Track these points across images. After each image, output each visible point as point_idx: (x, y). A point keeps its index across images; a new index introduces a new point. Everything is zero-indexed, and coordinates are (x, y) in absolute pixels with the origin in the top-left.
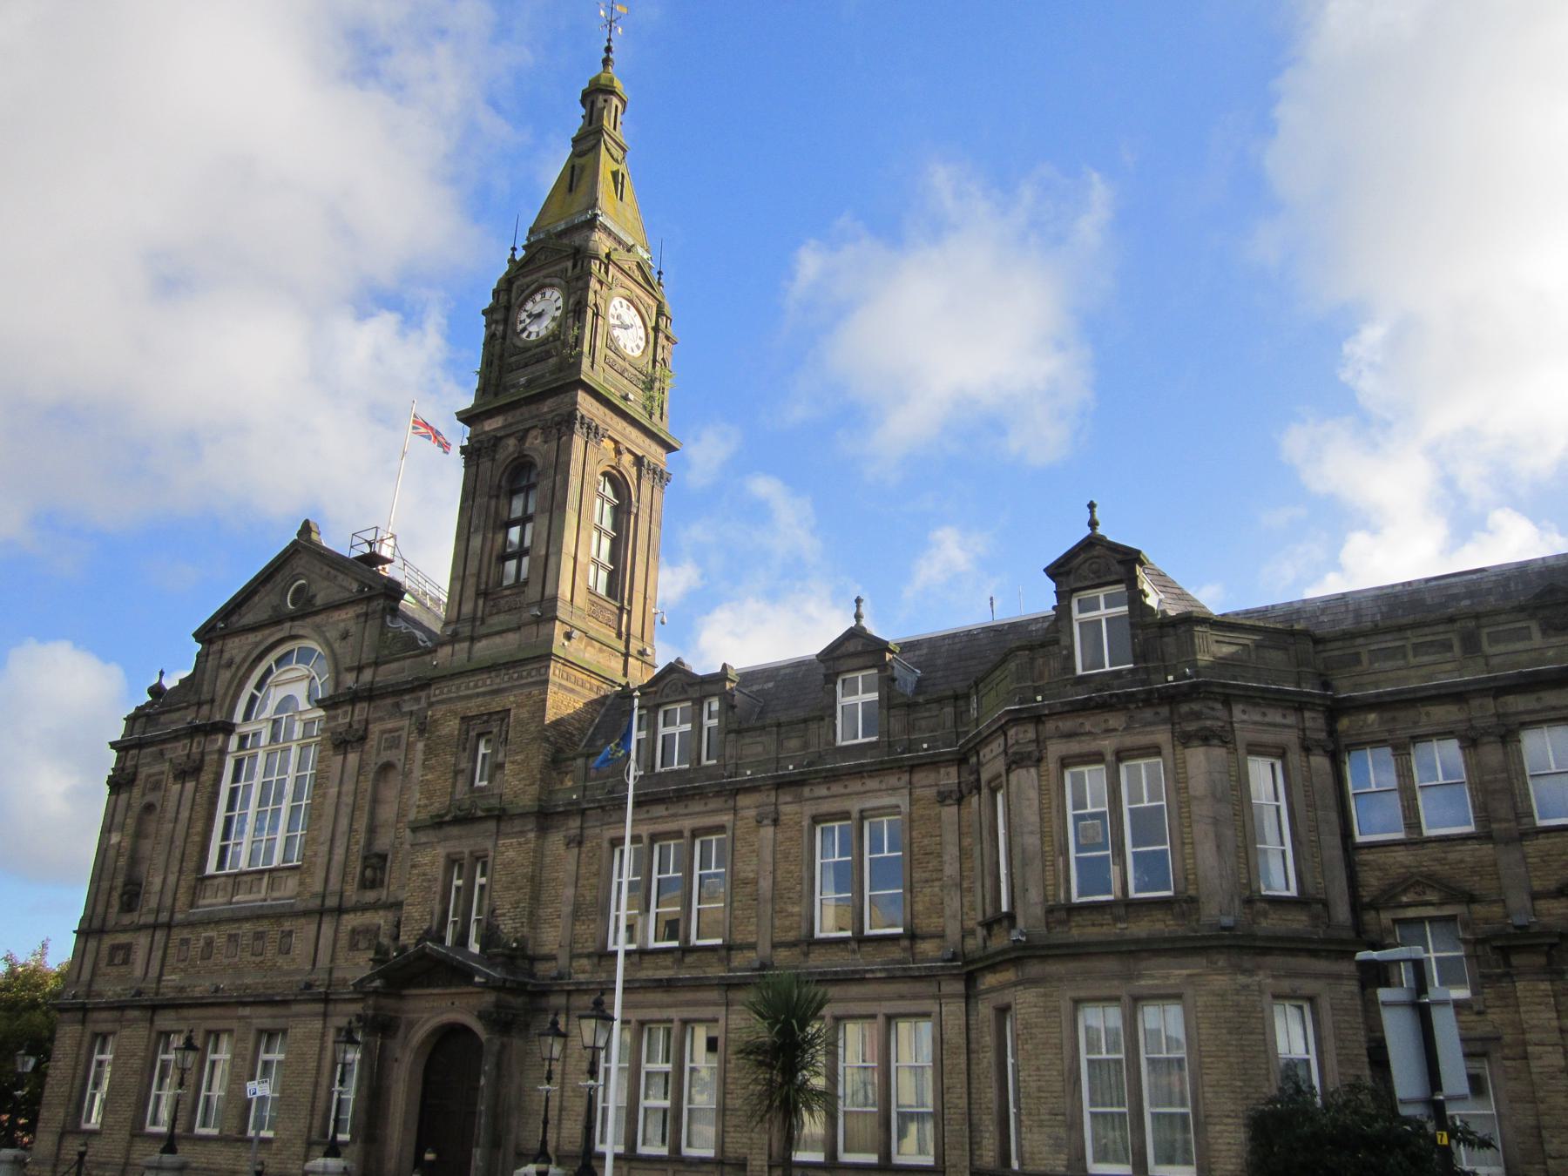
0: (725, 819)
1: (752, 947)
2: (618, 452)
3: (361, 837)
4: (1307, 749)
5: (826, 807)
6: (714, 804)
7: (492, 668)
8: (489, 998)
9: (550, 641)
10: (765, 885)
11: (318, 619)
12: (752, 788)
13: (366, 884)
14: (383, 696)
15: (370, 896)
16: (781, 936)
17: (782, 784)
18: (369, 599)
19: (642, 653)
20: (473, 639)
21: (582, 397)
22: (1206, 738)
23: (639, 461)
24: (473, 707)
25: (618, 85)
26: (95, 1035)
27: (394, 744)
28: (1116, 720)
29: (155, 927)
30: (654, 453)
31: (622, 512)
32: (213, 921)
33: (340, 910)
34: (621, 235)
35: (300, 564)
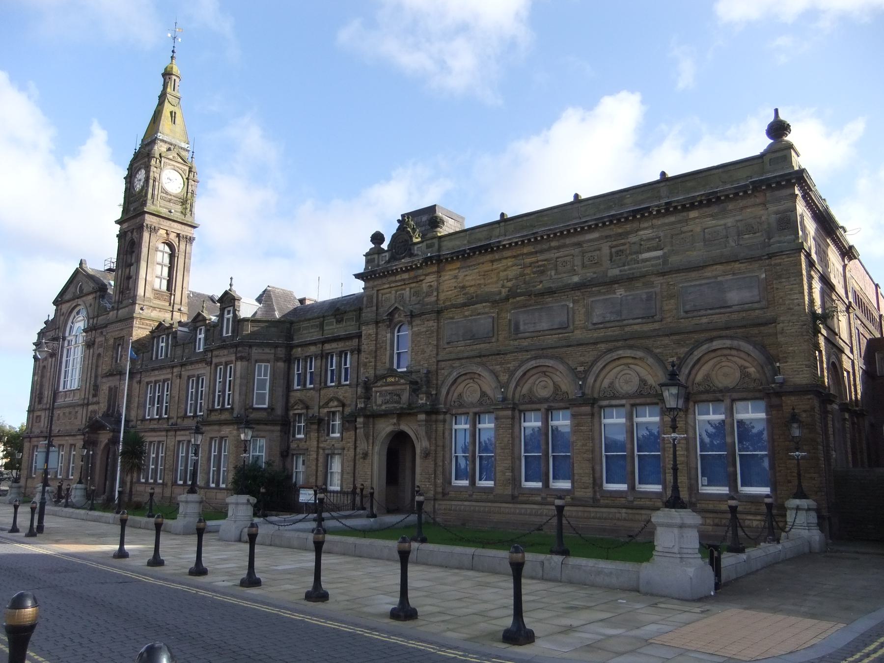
0: (170, 376)
1: (173, 418)
2: (167, 234)
3: (93, 379)
4: (277, 359)
5: (191, 373)
6: (169, 370)
7: (120, 321)
8: (111, 434)
9: (134, 312)
10: (177, 398)
11: (84, 298)
12: (176, 366)
13: (95, 396)
14: (99, 329)
15: (95, 399)
16: (180, 415)
17: (182, 365)
18: (96, 292)
19: (179, 310)
20: (118, 310)
21: (147, 216)
22: (241, 359)
23: (178, 235)
24: (116, 334)
25: (176, 70)
26: (34, 446)
27: (101, 346)
28: (226, 352)
29: (45, 409)
30: (186, 231)
31: (172, 256)
32: (60, 408)
33: (88, 404)
34: (173, 141)
35: (80, 277)
